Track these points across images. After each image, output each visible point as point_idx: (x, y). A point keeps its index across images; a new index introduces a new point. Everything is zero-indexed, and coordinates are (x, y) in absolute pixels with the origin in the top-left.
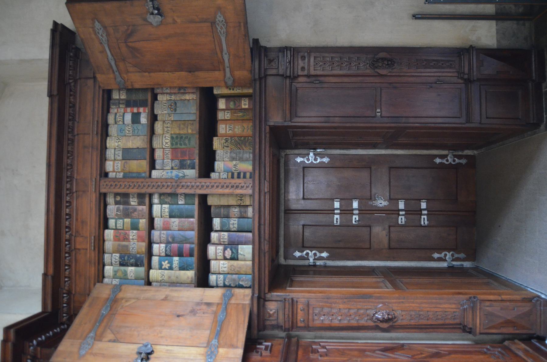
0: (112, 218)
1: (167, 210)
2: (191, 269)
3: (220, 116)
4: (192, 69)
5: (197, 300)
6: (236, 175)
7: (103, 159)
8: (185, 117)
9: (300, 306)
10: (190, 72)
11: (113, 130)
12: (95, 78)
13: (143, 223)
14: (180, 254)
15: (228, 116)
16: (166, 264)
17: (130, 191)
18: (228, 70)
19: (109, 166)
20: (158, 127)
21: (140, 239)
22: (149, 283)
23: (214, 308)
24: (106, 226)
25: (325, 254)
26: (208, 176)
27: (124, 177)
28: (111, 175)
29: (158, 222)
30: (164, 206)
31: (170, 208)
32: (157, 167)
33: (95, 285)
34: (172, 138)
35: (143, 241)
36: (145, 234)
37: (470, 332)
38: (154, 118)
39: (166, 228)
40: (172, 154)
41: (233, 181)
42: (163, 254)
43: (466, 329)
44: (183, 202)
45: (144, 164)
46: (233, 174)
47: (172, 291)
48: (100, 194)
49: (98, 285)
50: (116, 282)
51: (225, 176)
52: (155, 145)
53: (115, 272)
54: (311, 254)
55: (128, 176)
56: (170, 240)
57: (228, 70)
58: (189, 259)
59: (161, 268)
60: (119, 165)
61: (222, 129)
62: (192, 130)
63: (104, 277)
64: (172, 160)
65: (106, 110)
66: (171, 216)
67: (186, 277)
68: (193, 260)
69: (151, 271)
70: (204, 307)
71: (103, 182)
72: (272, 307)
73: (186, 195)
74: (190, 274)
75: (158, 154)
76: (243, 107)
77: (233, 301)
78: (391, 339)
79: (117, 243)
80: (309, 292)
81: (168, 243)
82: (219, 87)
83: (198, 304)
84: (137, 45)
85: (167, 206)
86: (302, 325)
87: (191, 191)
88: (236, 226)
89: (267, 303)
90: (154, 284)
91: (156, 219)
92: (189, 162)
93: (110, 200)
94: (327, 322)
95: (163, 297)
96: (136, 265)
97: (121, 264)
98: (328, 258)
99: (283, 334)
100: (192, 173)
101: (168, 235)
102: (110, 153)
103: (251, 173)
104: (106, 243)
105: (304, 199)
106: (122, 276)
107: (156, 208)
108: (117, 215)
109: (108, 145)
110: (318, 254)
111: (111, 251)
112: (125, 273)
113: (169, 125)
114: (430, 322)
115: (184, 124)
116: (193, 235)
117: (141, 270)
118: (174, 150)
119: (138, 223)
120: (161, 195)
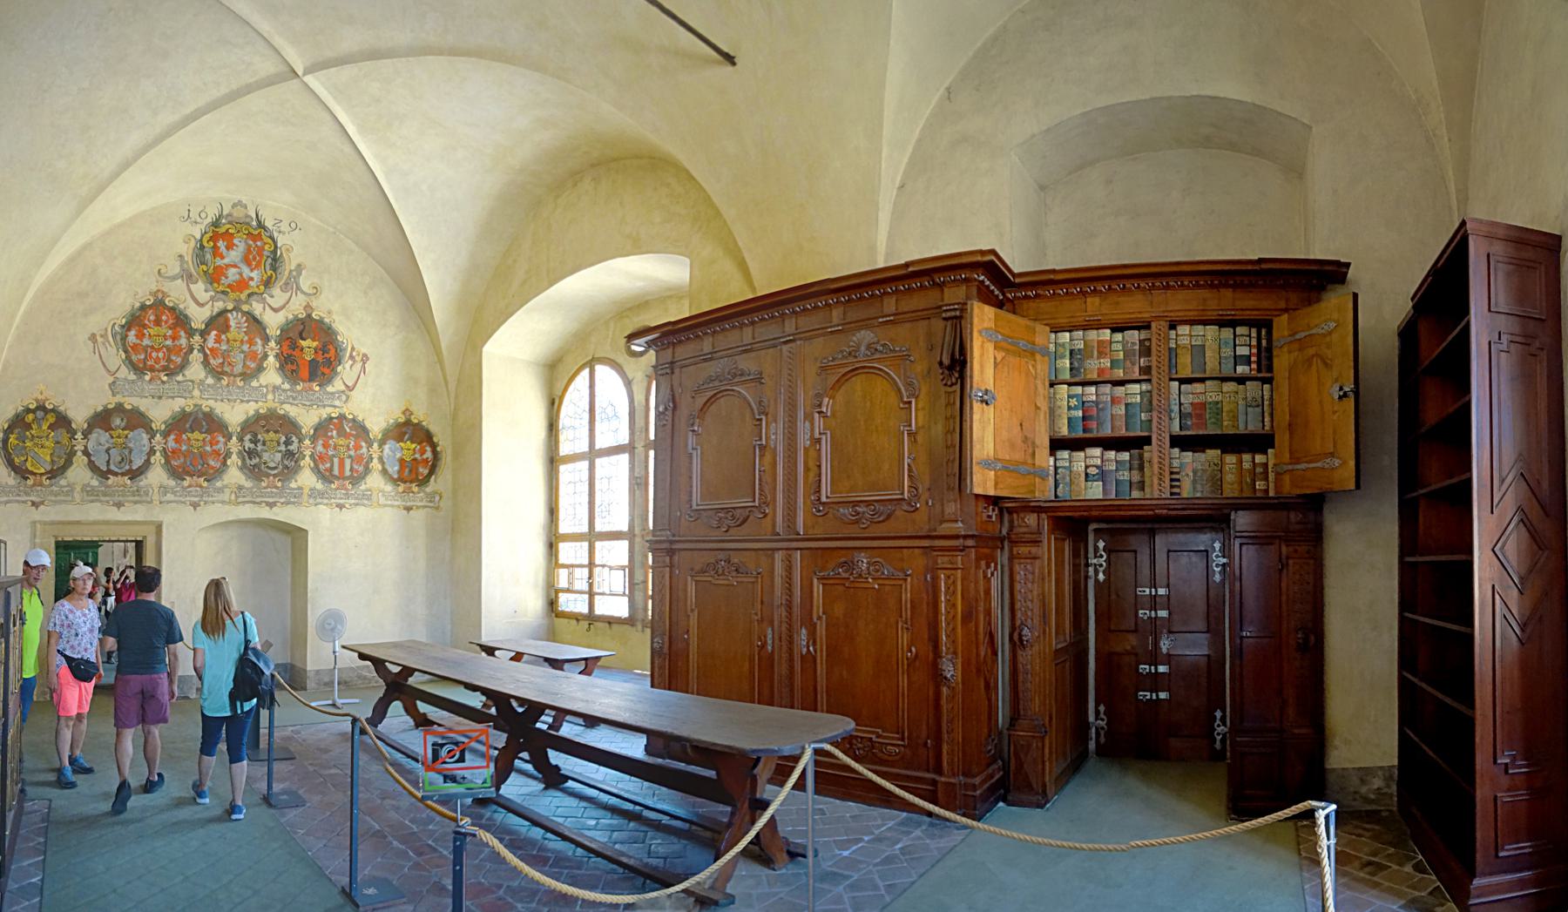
0: (1123, 338)
1: (1134, 400)
2: (1069, 431)
3: (1246, 457)
4: (1291, 426)
5: (1038, 442)
6: (1174, 476)
7: (1192, 323)
8: (1241, 419)
9: (1034, 550)
10: (1290, 425)
11: (1227, 333)
12: (1286, 310)
13: (1119, 374)
14: (1084, 418)
15: (1246, 466)
16: (1074, 402)
17: (1154, 358)
18: (1290, 467)
19: (1184, 330)
20: (1229, 387)
21: (1101, 371)
22: (1052, 385)
23: (1030, 461)
24: (1114, 330)
25: (1101, 577)
26: (1172, 446)
27: (1170, 349)
28: (1173, 333)
29: (1120, 390)
30: (1139, 396)
31: (1136, 403)
32: (1183, 386)
33: (1046, 325)
34: (1217, 403)
35: (1099, 376)
36: (1107, 377)
37: (1011, 725)
38: (1241, 380)
39: (1114, 401)
40: (1197, 404)
41: (1167, 474)
42: (1085, 399)
43: (1014, 718)
44: (1143, 418)
45: (1186, 373)
46: (1178, 473)
47: (1045, 413)
48: (1150, 322)
49: (1048, 329)
50: (1052, 347)
51: (1175, 465)
52: (1208, 383)
53: (1063, 345)
54: (1102, 561)
55: (1173, 353)
56: (1100, 406)
57: (1290, 467)
58: (1081, 428)
59: (1069, 397)
60: (1185, 342)
61: (1231, 459)
62: (1227, 426)
63: (1056, 332)
64: (1192, 404)
65: (1249, 323)
66: (1126, 405)
67: (1061, 425)
68: (1080, 434)
69: (1066, 386)
70: (1030, 451)
71: (1164, 325)
72: (1031, 519)
73: (1150, 421)
74: (1064, 431)
75: (1198, 387)
76: (1257, 483)
77: (1037, 480)
78: (1003, 644)
79: (1096, 345)
80: (1049, 559)
81: (1097, 403)
82: (1276, 455)
83: (1033, 443)
84: (1314, 367)
85: (1138, 399)
86: (1015, 553)
87: (1154, 429)
88: (1122, 478)
89: (1036, 515)
90: (1052, 390)
91: (1123, 388)
92: (1189, 423)
93: (1144, 334)
94: (1018, 578)
95: (1039, 405)
96: (1071, 369)
97: (1072, 352)
98: (1097, 580)
99: (1004, 532)
100: (1176, 429)
101: (1106, 402)
102: (1199, 329)
103: (1179, 494)
104: (1095, 332)
105: (1169, 551)
106: (1058, 353)
107: (1135, 388)
108: (1127, 342)
109: (1208, 327)
110: (1101, 569)
111: (1087, 338)
112: (1063, 357)
113: (1233, 398)
114: (1020, 684)
115: (1234, 416)
116: (1107, 432)
117: (1067, 376)
118: (1203, 405)
119: (1119, 368)
120: (1150, 392)
